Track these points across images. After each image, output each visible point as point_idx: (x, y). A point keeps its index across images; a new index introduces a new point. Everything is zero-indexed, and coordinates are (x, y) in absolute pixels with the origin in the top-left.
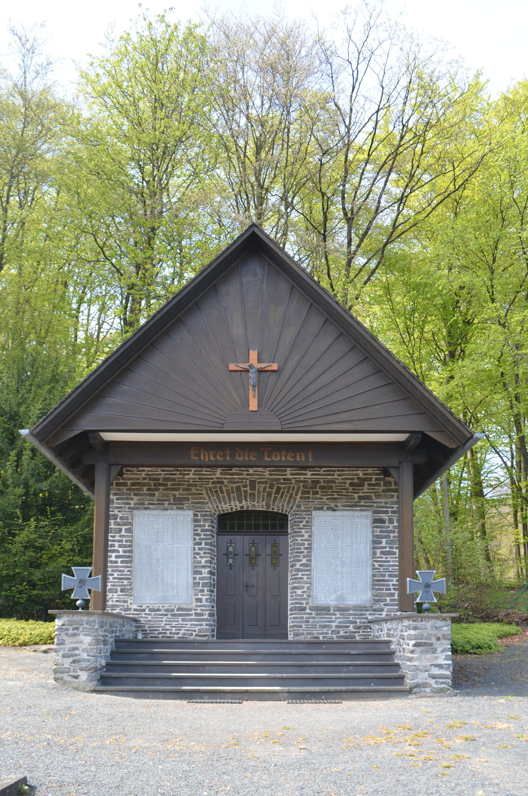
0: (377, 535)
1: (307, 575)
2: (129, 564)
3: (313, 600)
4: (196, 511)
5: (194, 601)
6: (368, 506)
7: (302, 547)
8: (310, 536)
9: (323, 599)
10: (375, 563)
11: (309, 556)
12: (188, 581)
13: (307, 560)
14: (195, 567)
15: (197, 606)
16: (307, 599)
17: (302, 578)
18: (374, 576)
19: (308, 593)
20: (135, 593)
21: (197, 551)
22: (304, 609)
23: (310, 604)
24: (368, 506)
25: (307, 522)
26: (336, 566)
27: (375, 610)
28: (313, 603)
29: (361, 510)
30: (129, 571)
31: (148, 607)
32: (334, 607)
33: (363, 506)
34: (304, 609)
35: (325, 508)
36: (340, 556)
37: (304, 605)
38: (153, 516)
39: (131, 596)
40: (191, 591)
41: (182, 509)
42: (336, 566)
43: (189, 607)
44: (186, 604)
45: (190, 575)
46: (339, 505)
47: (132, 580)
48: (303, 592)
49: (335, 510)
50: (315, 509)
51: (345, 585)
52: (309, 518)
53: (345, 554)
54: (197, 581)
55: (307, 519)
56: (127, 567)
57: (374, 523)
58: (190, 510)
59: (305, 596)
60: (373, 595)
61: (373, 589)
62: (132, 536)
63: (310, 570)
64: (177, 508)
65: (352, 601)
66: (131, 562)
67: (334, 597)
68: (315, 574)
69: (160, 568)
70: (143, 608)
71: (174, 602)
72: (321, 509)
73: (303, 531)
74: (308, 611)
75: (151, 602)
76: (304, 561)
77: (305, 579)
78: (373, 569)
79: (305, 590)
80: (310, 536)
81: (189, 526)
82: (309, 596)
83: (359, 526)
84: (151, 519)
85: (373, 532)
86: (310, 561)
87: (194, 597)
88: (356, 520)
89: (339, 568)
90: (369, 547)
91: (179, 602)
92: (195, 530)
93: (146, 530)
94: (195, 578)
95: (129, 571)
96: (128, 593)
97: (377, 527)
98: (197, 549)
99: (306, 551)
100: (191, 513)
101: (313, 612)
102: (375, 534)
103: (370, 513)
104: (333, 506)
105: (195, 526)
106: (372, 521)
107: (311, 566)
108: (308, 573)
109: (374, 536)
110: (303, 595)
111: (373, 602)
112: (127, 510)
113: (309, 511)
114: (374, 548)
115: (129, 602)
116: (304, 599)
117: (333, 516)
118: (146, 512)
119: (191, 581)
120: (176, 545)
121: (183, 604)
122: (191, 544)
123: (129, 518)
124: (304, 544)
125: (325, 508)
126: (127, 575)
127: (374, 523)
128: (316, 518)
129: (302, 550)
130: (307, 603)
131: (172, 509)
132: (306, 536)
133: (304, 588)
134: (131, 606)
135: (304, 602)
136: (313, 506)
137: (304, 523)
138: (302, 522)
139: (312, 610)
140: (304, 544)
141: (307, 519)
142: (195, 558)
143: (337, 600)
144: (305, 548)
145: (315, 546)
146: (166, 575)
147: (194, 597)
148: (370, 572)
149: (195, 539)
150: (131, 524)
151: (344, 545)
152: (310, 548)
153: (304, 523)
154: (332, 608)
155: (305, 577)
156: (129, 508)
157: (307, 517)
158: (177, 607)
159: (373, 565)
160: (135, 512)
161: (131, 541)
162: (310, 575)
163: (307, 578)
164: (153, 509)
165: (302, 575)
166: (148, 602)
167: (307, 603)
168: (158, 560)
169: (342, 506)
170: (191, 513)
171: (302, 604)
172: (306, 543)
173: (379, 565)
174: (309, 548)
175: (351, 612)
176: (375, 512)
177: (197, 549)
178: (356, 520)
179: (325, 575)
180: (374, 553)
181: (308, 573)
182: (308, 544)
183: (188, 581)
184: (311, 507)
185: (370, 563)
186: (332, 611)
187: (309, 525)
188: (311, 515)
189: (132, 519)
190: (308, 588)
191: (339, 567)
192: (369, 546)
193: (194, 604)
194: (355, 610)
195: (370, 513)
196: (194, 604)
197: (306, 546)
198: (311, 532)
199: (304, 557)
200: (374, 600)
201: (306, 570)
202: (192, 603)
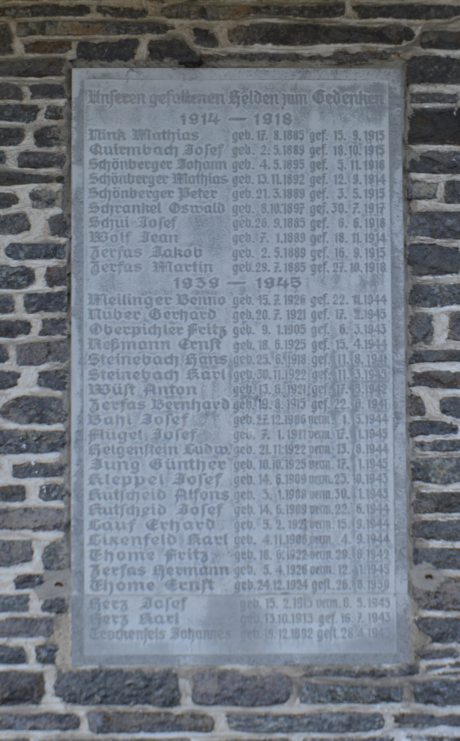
0: (429, 215)
1: (45, 470)
3: (78, 633)
6: (380, 35)
8: (61, 225)
9: (134, 624)
10: (421, 391)
11: (54, 350)
13: (45, 379)
16: (49, 627)
17: (18, 493)
18: (419, 471)
19: (48, 590)
23: (66, 659)
24: (380, 35)
25: (41, 137)
26: (209, 410)
28: (79, 648)
29: (341, 61)
32: (198, 677)
33: (350, 34)
35: (142, 51)
36: (226, 348)
37: (32, 666)
42: (209, 410)
46: (220, 28)
48: (24, 581)
50: (91, 54)
51: (258, 534)
52: (54, 113)
53: (257, 336)
55: (42, 120)
57: (414, 138)
59: (35, 609)
60: (420, 598)
61: (417, 557)
63: (60, 443)
65: (299, 636)
67: (196, 608)
72: (121, 53)
73: (23, 191)
74: (52, 703)
76: (28, 383)
77: (33, 500)
78: (414, 430)
79: (34, 567)
80: (61, 225)
82: (57, 606)
83: (332, 160)
85: (409, 198)
86: (57, 380)
88: (315, 123)
89: (225, 428)
90: (386, 289)
97: (430, 164)
99: (36, 320)
101: (81, 711)
102: (423, 205)
103: (388, 79)
104: (189, 38)
106: (403, 128)
107: (65, 417)
108: (50, 458)
109: (418, 222)
110: (23, 603)
113: (55, 67)
114: (418, 296)
116: (29, 627)
117: (186, 98)
124: (29, 276)
125: (142, 51)
127: (414, 138)
128: (90, 109)
129: (20, 313)
130: (48, 655)
132: (39, 223)
133: (27, 557)
135: (29, 644)
136: (76, 39)
137: (28, 143)
139: (72, 699)
140: (29, 276)
141: (42, 120)
143: (212, 629)
145: (87, 286)
148: (396, 454)
151: (251, 278)
153: (28, 143)
154: (185, 685)
155: (33, 485)
157: (43, 103)
159: (415, 405)
162: (60, 469)
163: (48, 493)
167: (48, 655)
169: (236, 35)
171: (19, 656)
172: (40, 266)
173: (448, 406)
174: (57, 302)
175: (295, 707)
176: (416, 72)
178: (315, 123)
179: (146, 472)
180: (420, 330)
181: (50, 458)
182: (52, 277)
184: (63, 45)
185: (394, 392)
186: (187, 705)
187: (51, 160)
188: (62, 91)
190: (52, 555)
191: (225, 418)
192: (389, 286)
194: (315, 694)
195: (388, 79)
197: (40, 286)
198: (67, 202)
199: (28, 356)
201: (38, 443)
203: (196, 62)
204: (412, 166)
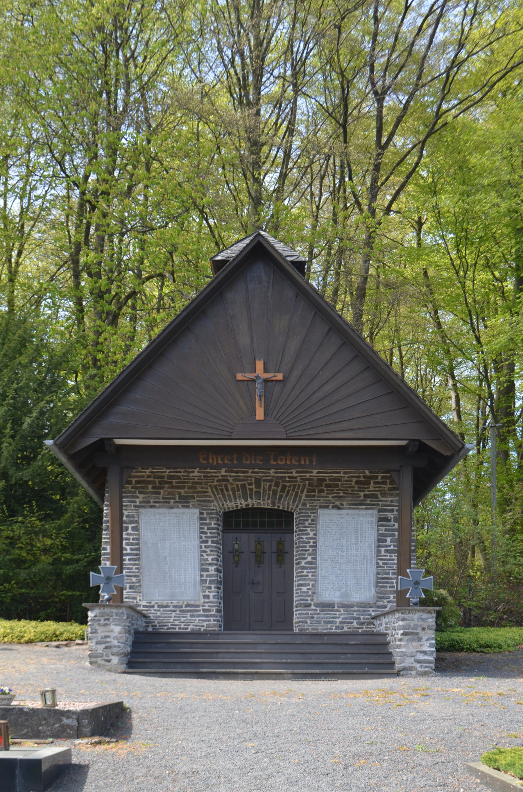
0: (382, 534)
1: (312, 572)
2: (136, 562)
3: (317, 597)
4: (202, 509)
5: (202, 597)
6: (374, 505)
7: (308, 546)
8: (315, 534)
9: (327, 596)
10: (379, 561)
11: (314, 554)
12: (195, 579)
13: (312, 558)
14: (202, 564)
15: (204, 602)
16: (312, 596)
17: (308, 576)
18: (378, 573)
19: (312, 590)
20: (144, 589)
21: (204, 549)
22: (309, 605)
23: (315, 601)
24: (374, 505)
25: (312, 520)
26: (341, 564)
27: (378, 607)
28: (317, 599)
29: (366, 509)
30: (137, 568)
31: (156, 603)
32: (338, 604)
33: (368, 504)
34: (309, 605)
35: (331, 507)
36: (345, 554)
37: (309, 602)
38: (159, 514)
39: (140, 592)
40: (199, 588)
41: (188, 507)
42: (341, 564)
43: (197, 603)
44: (194, 601)
45: (198, 573)
46: (345, 503)
47: (141, 578)
48: (308, 589)
49: (340, 509)
50: (321, 507)
51: (349, 583)
52: (314, 516)
53: (350, 552)
54: (205, 578)
55: (312, 518)
56: (135, 565)
57: (379, 521)
58: (196, 508)
59: (310, 593)
60: (377, 593)
61: (377, 586)
62: (139, 534)
63: (315, 568)
64: (183, 506)
65: (356, 598)
66: (139, 559)
67: (338, 593)
68: (320, 573)
69: (168, 566)
70: (152, 604)
71: (182, 598)
72: (327, 507)
73: (309, 529)
74: (313, 607)
75: (160, 598)
76: (309, 559)
77: (310, 577)
78: (377, 567)
79: (310, 587)
80: (315, 534)
81: (195, 524)
82: (314, 593)
83: (364, 525)
84: (158, 517)
85: (378, 531)
86: (315, 559)
87: (201, 594)
88: (361, 519)
89: (344, 566)
90: (373, 545)
91: (187, 598)
92: (201, 528)
93: (153, 528)
94: (202, 576)
95: (137, 568)
96: (137, 590)
97: (382, 525)
98: (203, 547)
99: (311, 549)
100: (197, 511)
101: (318, 609)
102: (380, 532)
103: (375, 512)
104: (339, 505)
105: (201, 524)
106: (377, 520)
107: (316, 564)
108: (313, 570)
109: (379, 535)
110: (308, 592)
111: (376, 599)
112: (133, 508)
113: (314, 509)
114: (379, 546)
115: (138, 598)
116: (309, 596)
117: (338, 514)
118: (152, 510)
119: (198, 578)
120: (183, 543)
121: (191, 600)
122: (197, 542)
123: (135, 516)
124: (310, 542)
125: (331, 507)
126: (135, 572)
127: (379, 521)
128: (321, 516)
129: (308, 548)
130: (312, 600)
131: (178, 507)
132: (311, 534)
133: (309, 585)
134: (140, 603)
135: (309, 599)
136: (318, 505)
137: (310, 521)
138: (307, 520)
139: (316, 607)
140: (310, 542)
141: (312, 518)
142: (202, 555)
143: (341, 597)
144: (310, 546)
145: (320, 544)
146: (173, 572)
147: (201, 594)
148: (374, 570)
149: (201, 537)
150: (137, 522)
151: (349, 543)
152: (316, 546)
153: (310, 521)
154: (336, 605)
155: (310, 575)
156: (135, 506)
157: (312, 515)
158: (185, 603)
159: (378, 563)
160: (141, 510)
161: (138, 539)
162: (315, 572)
163: (312, 576)
164: (159, 507)
165: (307, 572)
166: (157, 598)
167: (312, 600)
168: (165, 558)
169: (347, 504)
170: (197, 511)
171: (307, 600)
172: (311, 541)
173: (383, 564)
174: (315, 546)
175: (355, 609)
176: (380, 511)
177: (203, 547)
178: (361, 519)
179: (330, 573)
180: (379, 552)
181: (313, 570)
182: (313, 543)
183: (195, 579)
184: (316, 506)
185: (374, 561)
186: (336, 608)
187: (314, 523)
188: (316, 513)
189: (138, 517)
190: (313, 585)
191: (344, 565)
192: (374, 545)
193: (202, 600)
194: (358, 607)
195: (375, 512)
196: (202, 600)
197: (311, 544)
198: (316, 531)
199: (309, 555)
200: (378, 597)
201: (311, 568)
202: (199, 600)
203: (340, 509)
204: (379, 526)
